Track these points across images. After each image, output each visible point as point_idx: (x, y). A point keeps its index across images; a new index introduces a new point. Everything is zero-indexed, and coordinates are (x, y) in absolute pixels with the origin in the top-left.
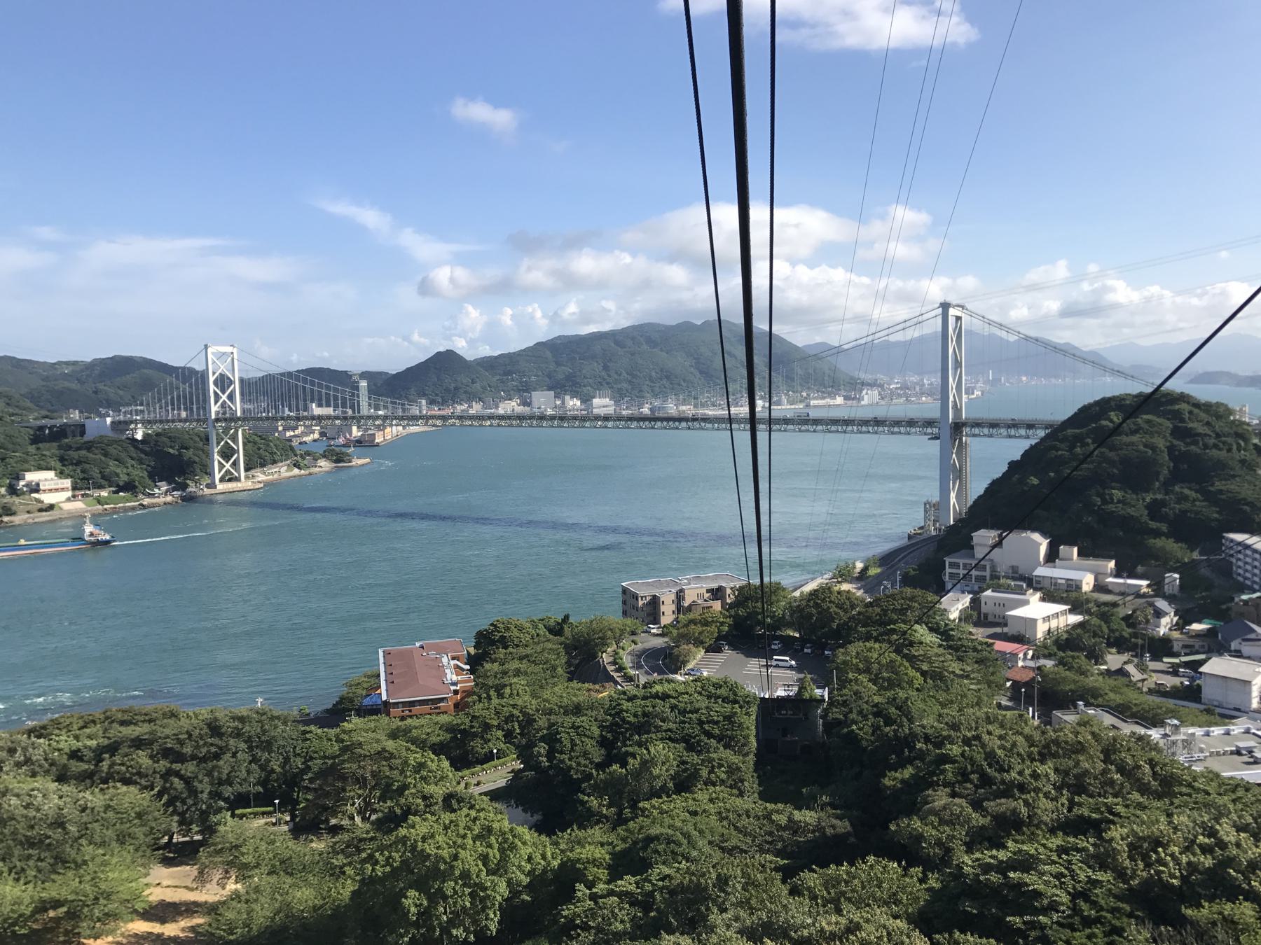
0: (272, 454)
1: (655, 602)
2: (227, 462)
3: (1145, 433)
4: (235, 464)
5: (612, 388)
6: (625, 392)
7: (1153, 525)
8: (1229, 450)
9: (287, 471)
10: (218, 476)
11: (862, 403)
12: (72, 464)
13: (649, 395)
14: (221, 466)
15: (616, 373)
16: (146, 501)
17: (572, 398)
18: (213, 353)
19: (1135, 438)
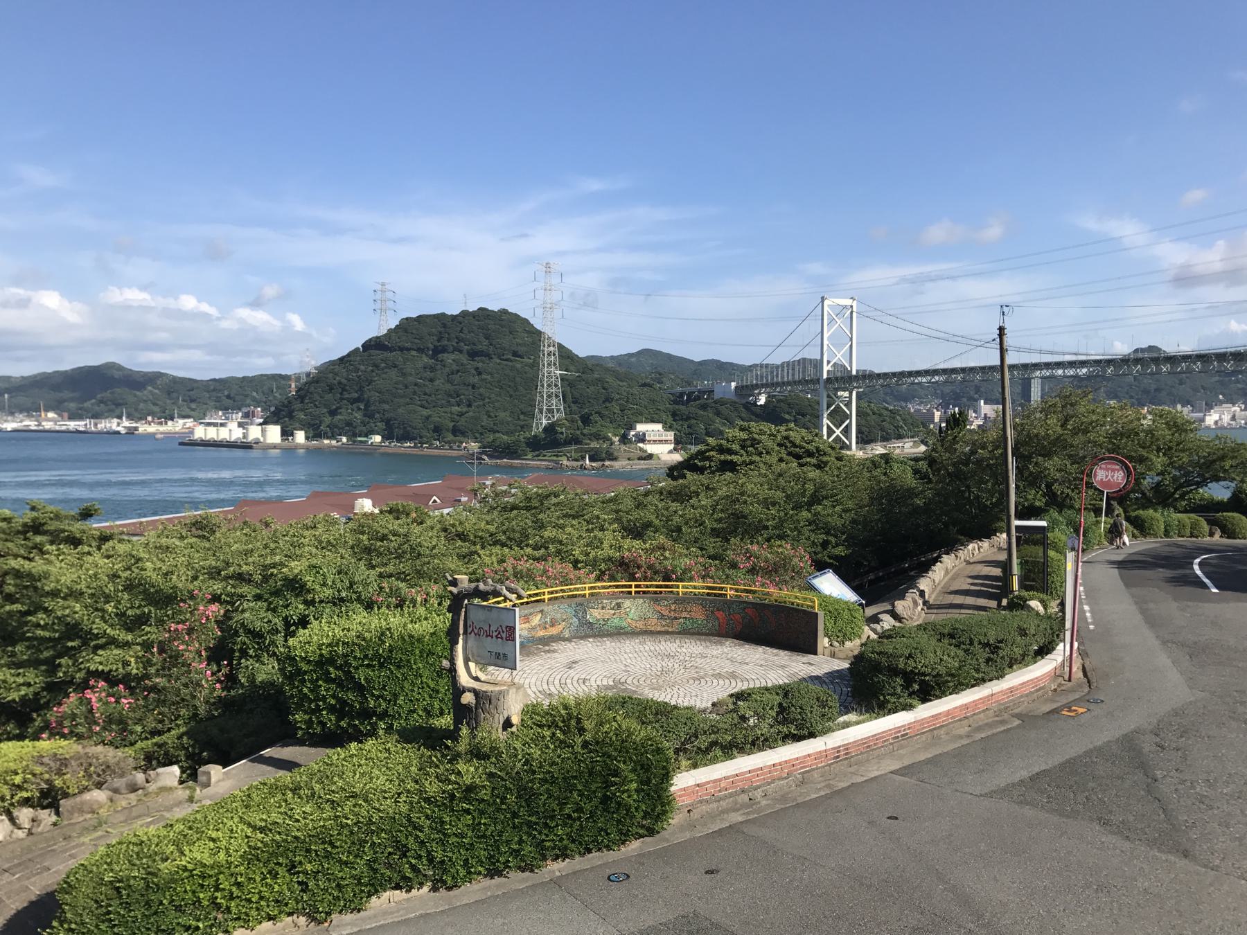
0: (897, 427)
4: (846, 431)
18: (828, 305)
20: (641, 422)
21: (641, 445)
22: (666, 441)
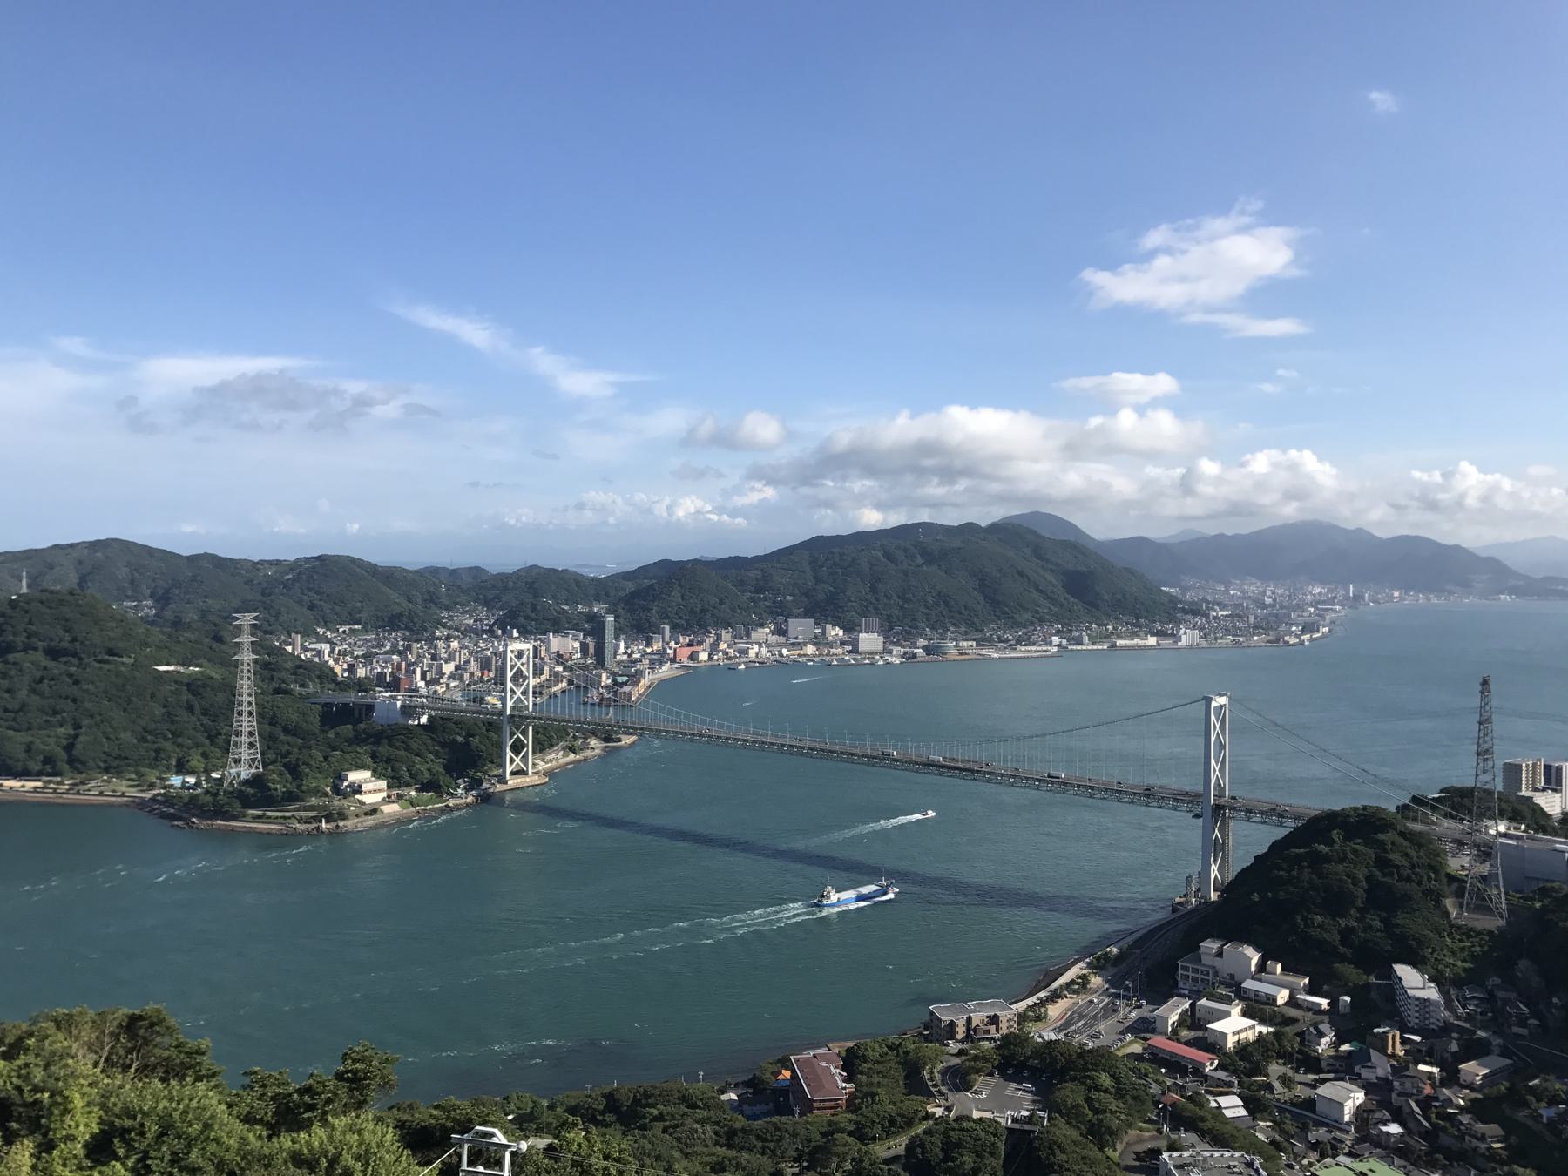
1: (952, 1024)
2: (517, 757)
3: (1351, 863)
4: (525, 757)
6: (895, 620)
7: (1342, 949)
8: (1419, 884)
9: (563, 756)
10: (508, 771)
14: (512, 761)
15: (886, 596)
17: (834, 625)
19: (1340, 867)
20: (350, 770)
21: (357, 797)
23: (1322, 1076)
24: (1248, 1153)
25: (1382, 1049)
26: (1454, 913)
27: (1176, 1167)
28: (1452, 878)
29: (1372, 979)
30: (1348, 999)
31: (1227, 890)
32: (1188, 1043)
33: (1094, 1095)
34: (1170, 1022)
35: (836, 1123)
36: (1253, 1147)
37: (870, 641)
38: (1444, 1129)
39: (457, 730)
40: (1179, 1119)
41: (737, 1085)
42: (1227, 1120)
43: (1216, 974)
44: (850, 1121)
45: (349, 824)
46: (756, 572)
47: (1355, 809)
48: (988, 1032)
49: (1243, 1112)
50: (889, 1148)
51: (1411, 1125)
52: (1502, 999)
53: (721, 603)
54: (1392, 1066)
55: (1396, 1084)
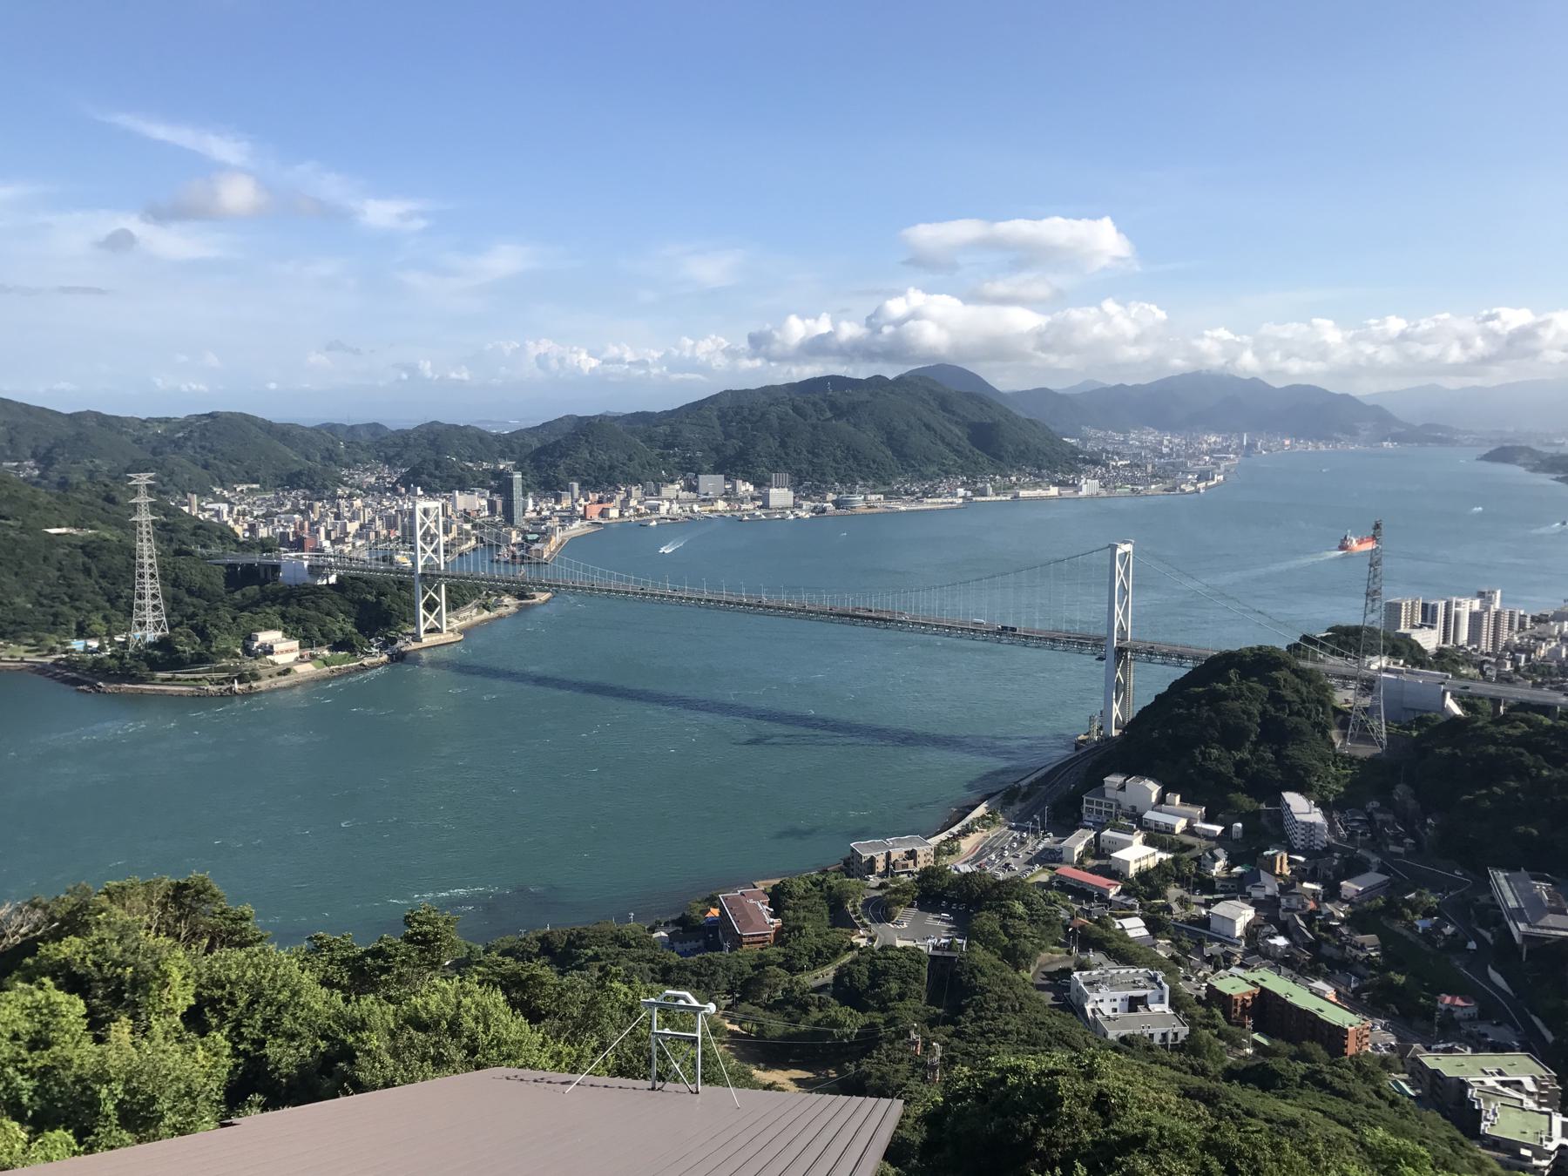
1: (872, 860)
4: (439, 615)
5: (791, 468)
7: (1236, 781)
8: (1309, 717)
9: (478, 614)
10: (422, 629)
11: (1080, 493)
12: (292, 621)
13: (832, 479)
14: (425, 619)
15: (795, 451)
16: (367, 661)
17: (744, 481)
19: (1237, 704)
21: (269, 657)
22: (292, 651)
23: (1216, 896)
24: (1152, 970)
25: (1271, 870)
26: (1338, 743)
27: (1085, 984)
28: (1337, 711)
29: (1263, 806)
30: (1240, 825)
31: (1133, 728)
32: (1093, 871)
33: (1009, 922)
34: (1076, 852)
35: (766, 957)
36: (1155, 963)
37: (780, 496)
38: (1327, 941)
39: (366, 590)
40: (1088, 941)
41: (666, 924)
42: (1130, 941)
43: (1119, 806)
44: (779, 954)
45: (263, 685)
46: (665, 427)
47: (1251, 649)
48: (906, 866)
49: (1145, 932)
50: (817, 978)
51: (1296, 937)
52: (1381, 821)
53: (630, 459)
54: (1280, 885)
55: (1283, 901)
